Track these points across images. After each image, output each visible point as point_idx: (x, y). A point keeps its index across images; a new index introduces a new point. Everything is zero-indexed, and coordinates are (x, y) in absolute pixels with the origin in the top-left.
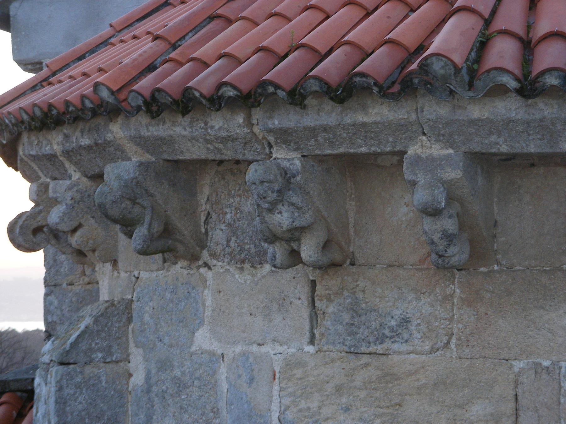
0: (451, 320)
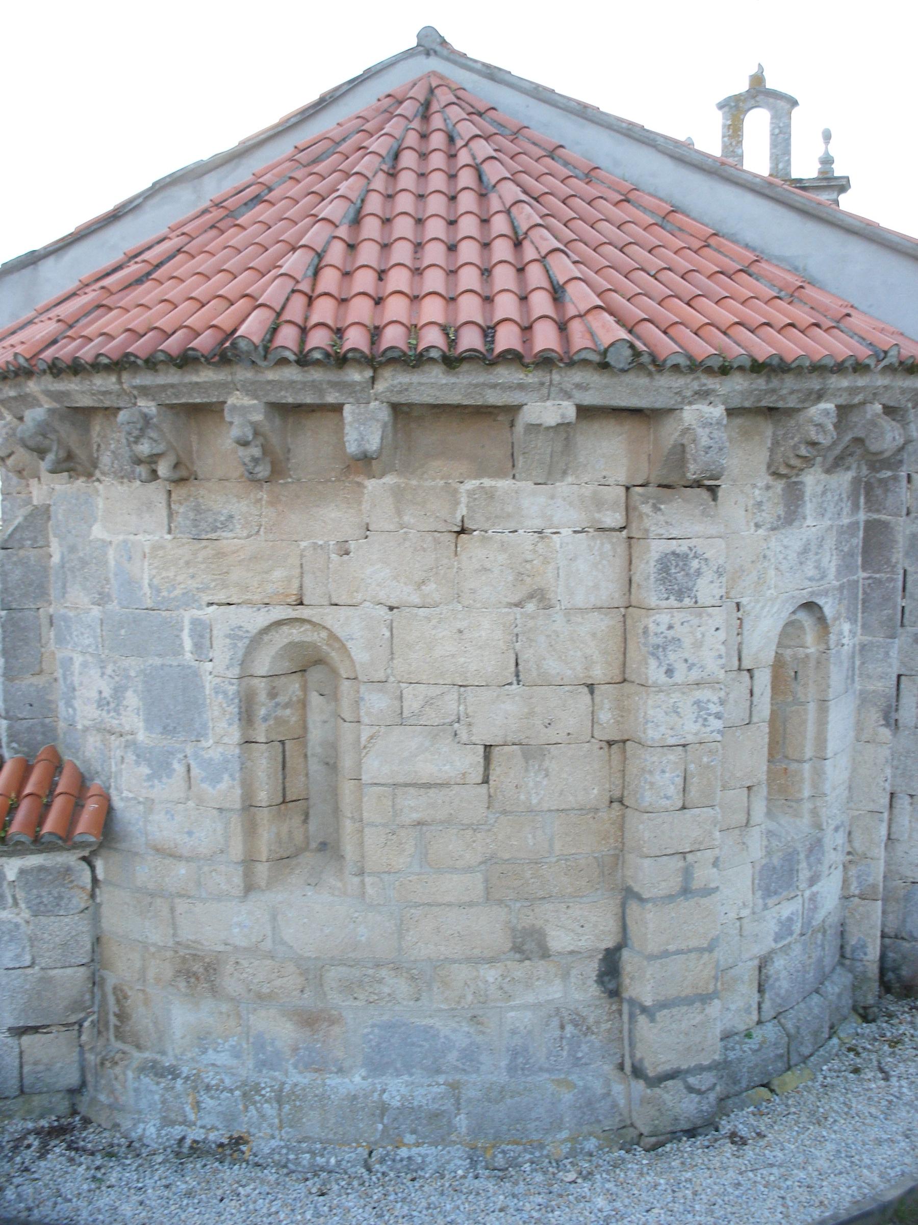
0: (260, 515)
